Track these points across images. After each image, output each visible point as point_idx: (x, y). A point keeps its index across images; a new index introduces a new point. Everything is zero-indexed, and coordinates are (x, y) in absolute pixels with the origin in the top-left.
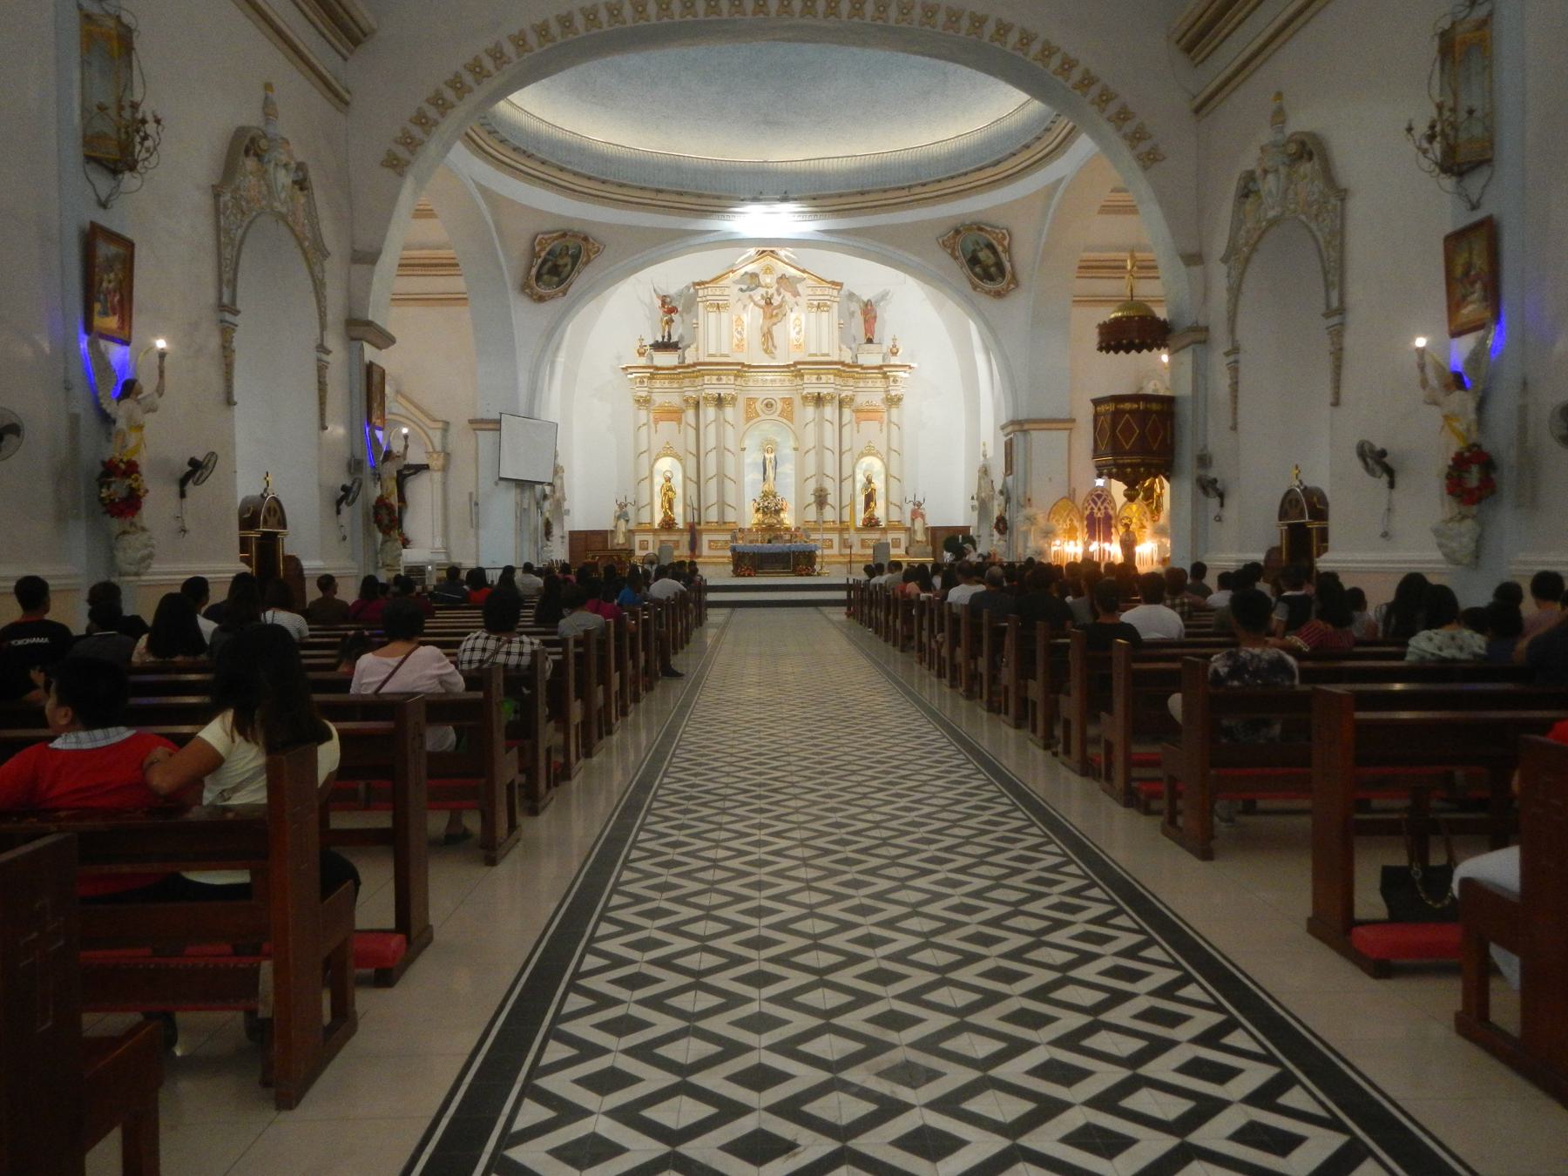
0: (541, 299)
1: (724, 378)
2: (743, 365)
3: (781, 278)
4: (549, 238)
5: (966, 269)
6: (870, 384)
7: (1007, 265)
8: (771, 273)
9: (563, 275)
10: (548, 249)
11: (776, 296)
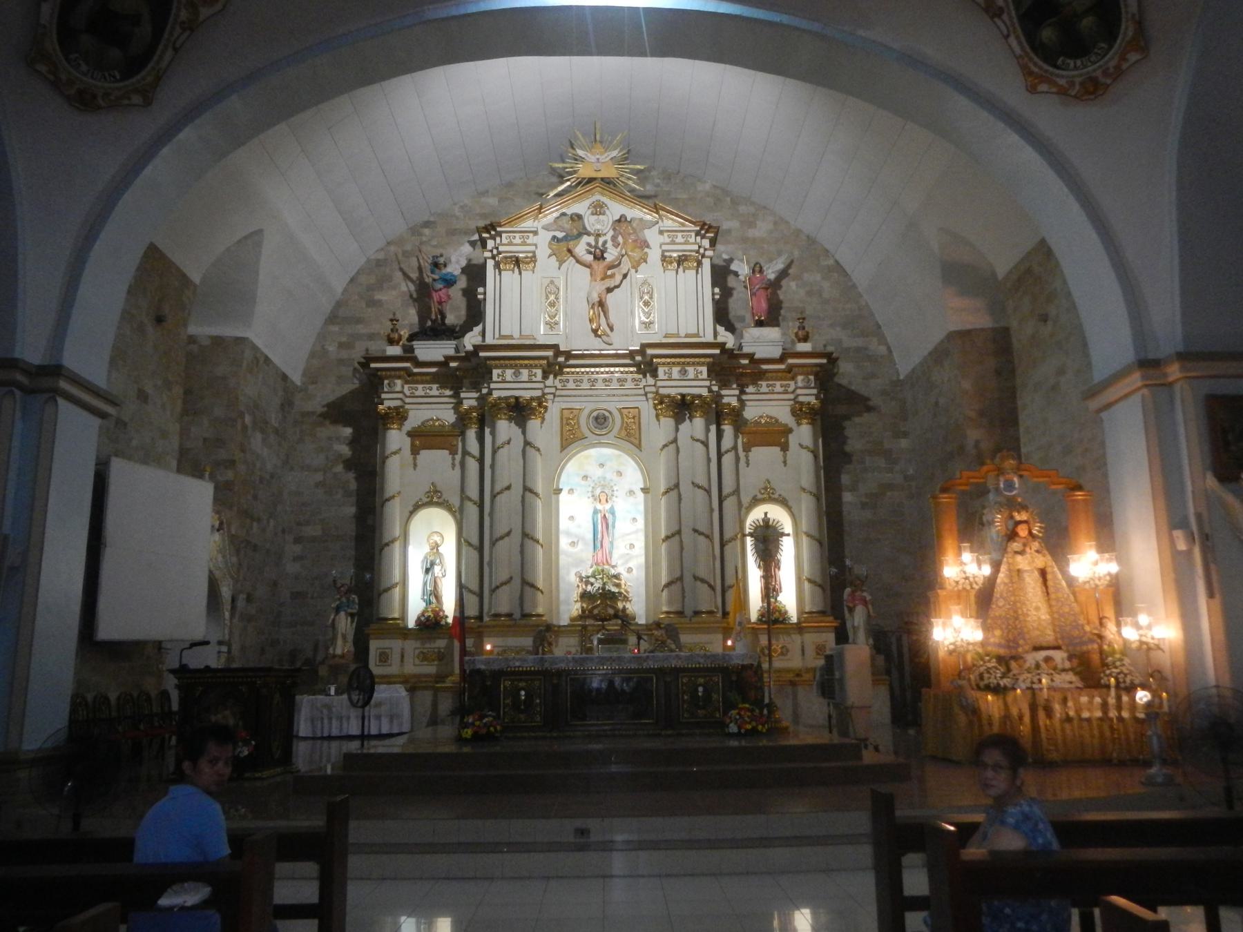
0: (85, 101)
1: (525, 372)
2: (555, 347)
3: (619, 221)
6: (764, 389)
8: (604, 214)
11: (609, 244)
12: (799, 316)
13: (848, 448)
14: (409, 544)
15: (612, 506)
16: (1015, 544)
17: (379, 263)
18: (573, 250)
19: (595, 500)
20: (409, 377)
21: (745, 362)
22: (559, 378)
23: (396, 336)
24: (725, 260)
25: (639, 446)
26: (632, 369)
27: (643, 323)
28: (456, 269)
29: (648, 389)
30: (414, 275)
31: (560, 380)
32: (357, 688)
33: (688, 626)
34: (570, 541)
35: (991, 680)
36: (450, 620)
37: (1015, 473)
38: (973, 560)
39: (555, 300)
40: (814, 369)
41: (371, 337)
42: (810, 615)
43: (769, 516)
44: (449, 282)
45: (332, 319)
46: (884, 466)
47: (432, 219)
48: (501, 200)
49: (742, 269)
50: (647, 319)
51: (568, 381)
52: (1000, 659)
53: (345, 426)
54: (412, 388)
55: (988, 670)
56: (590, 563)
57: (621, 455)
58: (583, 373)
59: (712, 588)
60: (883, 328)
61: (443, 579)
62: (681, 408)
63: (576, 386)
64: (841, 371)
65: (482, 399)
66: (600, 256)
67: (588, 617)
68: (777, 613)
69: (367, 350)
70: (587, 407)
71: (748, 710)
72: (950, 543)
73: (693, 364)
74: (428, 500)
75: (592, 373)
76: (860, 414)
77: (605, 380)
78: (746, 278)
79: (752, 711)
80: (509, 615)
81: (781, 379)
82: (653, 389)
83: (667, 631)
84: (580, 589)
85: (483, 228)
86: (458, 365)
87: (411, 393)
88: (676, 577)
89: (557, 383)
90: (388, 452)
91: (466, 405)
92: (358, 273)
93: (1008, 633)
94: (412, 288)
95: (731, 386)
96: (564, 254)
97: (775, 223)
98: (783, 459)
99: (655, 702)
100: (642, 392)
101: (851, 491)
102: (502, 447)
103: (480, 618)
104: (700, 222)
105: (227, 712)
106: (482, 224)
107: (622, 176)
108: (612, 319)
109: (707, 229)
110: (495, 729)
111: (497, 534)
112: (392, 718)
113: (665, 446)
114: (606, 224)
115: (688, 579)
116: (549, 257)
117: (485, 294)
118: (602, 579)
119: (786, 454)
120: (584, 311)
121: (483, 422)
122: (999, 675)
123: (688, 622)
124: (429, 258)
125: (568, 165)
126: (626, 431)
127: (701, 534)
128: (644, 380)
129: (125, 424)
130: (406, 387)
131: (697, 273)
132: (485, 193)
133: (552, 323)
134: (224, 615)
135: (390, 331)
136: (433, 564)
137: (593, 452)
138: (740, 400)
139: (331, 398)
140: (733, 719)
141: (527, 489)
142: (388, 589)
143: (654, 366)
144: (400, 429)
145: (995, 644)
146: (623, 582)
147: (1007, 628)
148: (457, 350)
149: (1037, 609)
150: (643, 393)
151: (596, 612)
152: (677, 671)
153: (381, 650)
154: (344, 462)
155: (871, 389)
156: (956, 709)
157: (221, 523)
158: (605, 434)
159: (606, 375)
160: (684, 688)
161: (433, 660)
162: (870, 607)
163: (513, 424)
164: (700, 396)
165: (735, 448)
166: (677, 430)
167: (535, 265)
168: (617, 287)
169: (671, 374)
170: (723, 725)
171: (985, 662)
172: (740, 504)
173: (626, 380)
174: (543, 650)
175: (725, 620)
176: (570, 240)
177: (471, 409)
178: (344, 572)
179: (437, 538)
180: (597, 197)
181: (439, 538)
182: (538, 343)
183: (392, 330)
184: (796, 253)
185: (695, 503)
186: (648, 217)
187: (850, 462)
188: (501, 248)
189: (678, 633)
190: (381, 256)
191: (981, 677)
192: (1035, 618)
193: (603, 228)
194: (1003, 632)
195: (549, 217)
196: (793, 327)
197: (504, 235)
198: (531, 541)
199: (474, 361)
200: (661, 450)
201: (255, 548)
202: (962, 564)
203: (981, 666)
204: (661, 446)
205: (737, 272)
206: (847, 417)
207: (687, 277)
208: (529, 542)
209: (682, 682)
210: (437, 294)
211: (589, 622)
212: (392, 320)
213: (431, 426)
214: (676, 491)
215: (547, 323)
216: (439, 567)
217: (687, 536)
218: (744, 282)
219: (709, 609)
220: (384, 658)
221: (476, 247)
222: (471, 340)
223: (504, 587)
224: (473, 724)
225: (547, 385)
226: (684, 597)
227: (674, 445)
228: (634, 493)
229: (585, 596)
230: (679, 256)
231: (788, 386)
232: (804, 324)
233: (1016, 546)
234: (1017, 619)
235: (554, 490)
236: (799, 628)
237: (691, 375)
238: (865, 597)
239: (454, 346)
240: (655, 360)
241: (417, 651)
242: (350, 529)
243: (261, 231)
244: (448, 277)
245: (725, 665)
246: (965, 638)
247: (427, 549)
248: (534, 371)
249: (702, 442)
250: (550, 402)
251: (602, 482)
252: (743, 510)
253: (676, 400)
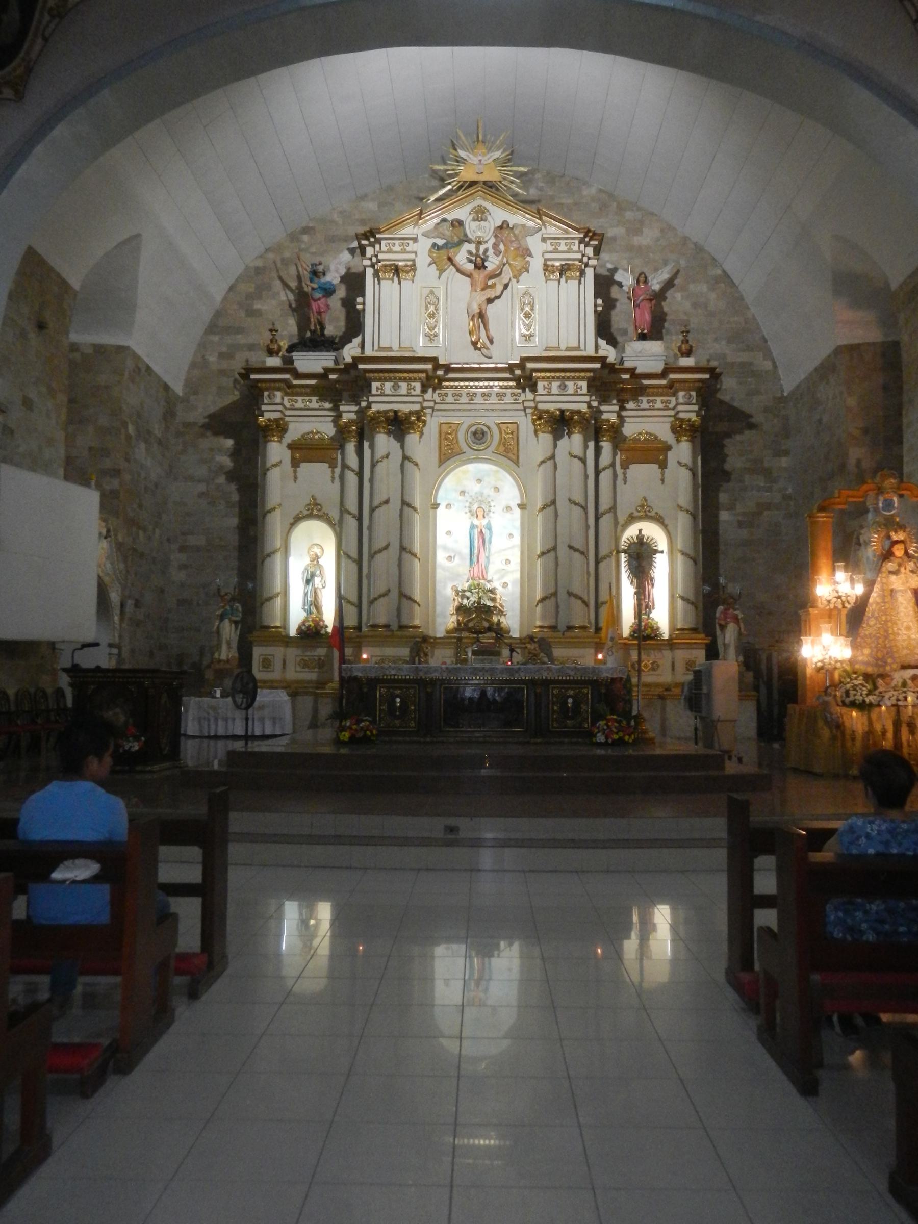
1: (404, 386)
2: (434, 360)
3: (501, 227)
6: (645, 405)
8: (485, 220)
11: (491, 252)
12: (683, 329)
13: (727, 467)
14: (290, 556)
15: (489, 521)
16: (890, 564)
17: (258, 271)
18: (453, 258)
19: (472, 515)
20: (289, 389)
21: (626, 376)
22: (438, 392)
23: (276, 347)
24: (609, 270)
25: (517, 462)
26: (511, 383)
27: (524, 336)
28: (335, 278)
29: (526, 404)
30: (293, 284)
31: (439, 394)
32: (241, 692)
33: (562, 640)
34: (447, 555)
35: (857, 697)
36: (330, 630)
37: (895, 492)
38: (846, 580)
39: (435, 311)
40: (697, 384)
41: (251, 347)
42: (682, 632)
43: (643, 533)
44: (329, 291)
45: (212, 328)
46: (762, 484)
47: (311, 225)
48: (381, 205)
49: (626, 279)
50: (528, 331)
51: (446, 395)
52: (867, 677)
53: (226, 437)
54: (292, 400)
55: (854, 688)
56: (466, 577)
57: (497, 471)
58: (462, 387)
59: (586, 604)
60: (769, 343)
61: (323, 590)
63: (455, 400)
64: (724, 387)
65: (361, 412)
66: (481, 265)
67: (463, 630)
68: (649, 630)
69: (247, 361)
70: (465, 421)
71: (616, 721)
72: (823, 563)
73: (574, 378)
74: (309, 512)
75: (471, 387)
76: (741, 432)
77: (484, 395)
78: (630, 289)
79: (619, 722)
80: (387, 626)
81: (661, 395)
82: (532, 404)
83: (539, 646)
84: (456, 602)
85: (363, 234)
86: (337, 378)
87: (291, 406)
88: (550, 592)
89: (436, 395)
90: (268, 465)
91: (345, 418)
92: (237, 280)
93: (877, 652)
94: (291, 297)
95: (611, 402)
96: (444, 262)
97: (662, 231)
98: (660, 476)
99: (525, 712)
100: (521, 407)
101: (728, 509)
102: (381, 461)
103: (359, 628)
104: (585, 228)
105: (118, 710)
106: (361, 230)
107: (505, 179)
108: (492, 332)
109: (590, 235)
110: (371, 732)
111: (378, 545)
112: (274, 720)
113: (543, 462)
114: (487, 231)
115: (562, 595)
116: (428, 266)
117: (364, 304)
118: (478, 593)
119: (664, 472)
120: (465, 323)
121: (360, 437)
122: (865, 692)
123: (561, 636)
124: (308, 267)
125: (450, 168)
126: (504, 445)
127: (576, 550)
128: (523, 395)
129: (12, 432)
130: (286, 398)
131: (580, 283)
132: (363, 197)
133: (431, 335)
134: (113, 620)
135: (269, 342)
136: (313, 575)
137: (471, 467)
138: (620, 416)
139: (212, 409)
140: (600, 729)
141: (406, 504)
142: (270, 599)
143: (534, 380)
144: (280, 441)
145: (863, 663)
146: (498, 597)
147: (876, 647)
148: (336, 362)
149: (908, 628)
150: (522, 408)
151: (471, 625)
152: (547, 683)
153: (264, 657)
154: (226, 473)
155: (753, 406)
156: (821, 723)
157: (108, 531)
158: (483, 450)
159: (485, 390)
160: (555, 699)
161: (314, 668)
162: (742, 625)
163: (391, 438)
164: (579, 412)
165: (613, 465)
166: (555, 446)
167: (415, 273)
168: (498, 297)
169: (550, 389)
170: (592, 735)
171: (851, 680)
172: (616, 522)
173: (504, 395)
174: (419, 660)
175: (598, 635)
176: (451, 248)
177: (351, 422)
178: (228, 580)
180: (479, 201)
181: (320, 550)
182: (417, 356)
183: (272, 341)
184: (683, 263)
185: (571, 519)
186: (531, 224)
187: (729, 481)
188: (380, 256)
189: (550, 647)
190: (259, 263)
191: (847, 693)
192: (905, 637)
193: (485, 235)
194: (872, 651)
195: (429, 223)
196: (676, 340)
197: (383, 242)
198: (409, 555)
199: (353, 373)
200: (539, 465)
201: (142, 555)
202: (836, 583)
203: (848, 683)
204: (538, 463)
205: (621, 282)
206: (728, 435)
207: (570, 287)
208: (406, 556)
209: (553, 694)
210: (316, 303)
211: (464, 634)
212: (271, 331)
213: (311, 439)
214: (552, 507)
215: (426, 335)
216: (320, 578)
217: (563, 551)
218: (628, 293)
219: (582, 624)
220: (267, 664)
221: (356, 255)
222: (350, 351)
223: (382, 599)
224: (350, 728)
225: (426, 398)
226: (557, 613)
227: (552, 461)
228: (511, 509)
229: (460, 609)
230: (562, 265)
231: (669, 402)
232: (687, 338)
233: (891, 565)
234: (886, 637)
235: (432, 505)
236: (670, 644)
237: (571, 390)
238: (737, 615)
239: (334, 358)
240: (534, 374)
241: (298, 659)
242: (233, 539)
243: (138, 236)
244: (327, 286)
245: (595, 678)
246: (833, 656)
247: (307, 561)
248: (413, 384)
249: (580, 459)
250: (429, 416)
251: (480, 498)
252: (619, 528)
253: (556, 416)
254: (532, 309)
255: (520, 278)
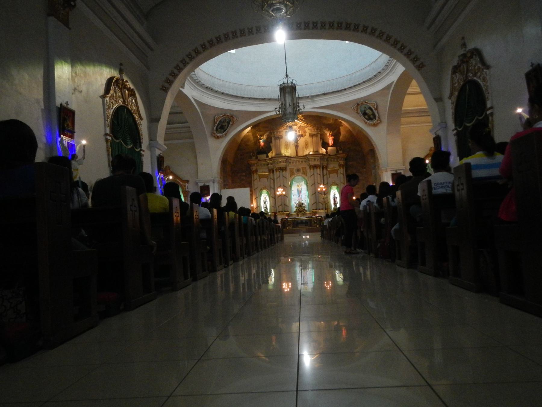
0: (218, 138)
3: (300, 127)
4: (220, 117)
5: (363, 117)
7: (377, 115)
8: (296, 125)
9: (225, 128)
10: (219, 121)
15: (301, 188)
62: (315, 167)
115: (318, 203)
127: (320, 193)
144: (256, 174)
151: (299, 210)
164: (318, 165)
179: (265, 196)
188: (275, 135)
197: (275, 132)
207: (315, 139)
230: (313, 135)
254: (307, 144)
255: (305, 137)
